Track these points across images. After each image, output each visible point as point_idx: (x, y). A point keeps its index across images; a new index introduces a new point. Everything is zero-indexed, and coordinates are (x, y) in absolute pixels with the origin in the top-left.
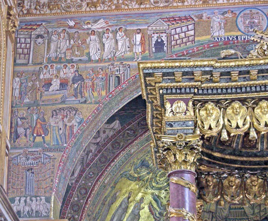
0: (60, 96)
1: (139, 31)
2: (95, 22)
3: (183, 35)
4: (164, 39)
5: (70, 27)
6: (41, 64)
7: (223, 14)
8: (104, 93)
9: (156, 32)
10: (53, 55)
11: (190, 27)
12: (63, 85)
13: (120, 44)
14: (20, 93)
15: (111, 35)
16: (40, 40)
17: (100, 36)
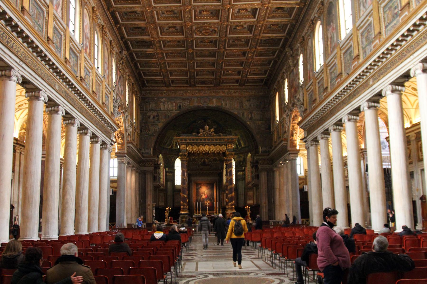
0: (153, 121)
1: (174, 102)
2: (163, 98)
3: (186, 104)
4: (181, 105)
5: (156, 100)
6: (147, 111)
7: (197, 98)
8: (165, 120)
9: (179, 103)
10: (151, 108)
11: (189, 102)
12: (154, 117)
13: (169, 106)
14: (142, 119)
15: (167, 103)
16: (147, 103)
17: (164, 103)
